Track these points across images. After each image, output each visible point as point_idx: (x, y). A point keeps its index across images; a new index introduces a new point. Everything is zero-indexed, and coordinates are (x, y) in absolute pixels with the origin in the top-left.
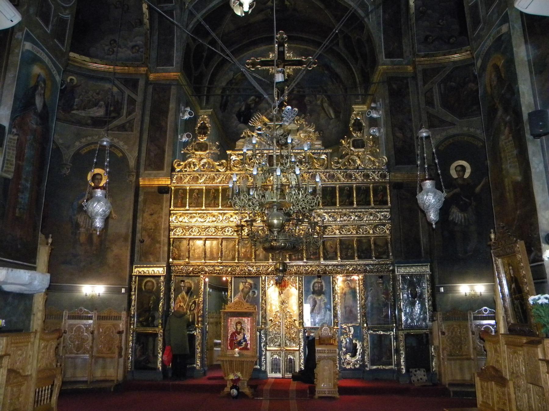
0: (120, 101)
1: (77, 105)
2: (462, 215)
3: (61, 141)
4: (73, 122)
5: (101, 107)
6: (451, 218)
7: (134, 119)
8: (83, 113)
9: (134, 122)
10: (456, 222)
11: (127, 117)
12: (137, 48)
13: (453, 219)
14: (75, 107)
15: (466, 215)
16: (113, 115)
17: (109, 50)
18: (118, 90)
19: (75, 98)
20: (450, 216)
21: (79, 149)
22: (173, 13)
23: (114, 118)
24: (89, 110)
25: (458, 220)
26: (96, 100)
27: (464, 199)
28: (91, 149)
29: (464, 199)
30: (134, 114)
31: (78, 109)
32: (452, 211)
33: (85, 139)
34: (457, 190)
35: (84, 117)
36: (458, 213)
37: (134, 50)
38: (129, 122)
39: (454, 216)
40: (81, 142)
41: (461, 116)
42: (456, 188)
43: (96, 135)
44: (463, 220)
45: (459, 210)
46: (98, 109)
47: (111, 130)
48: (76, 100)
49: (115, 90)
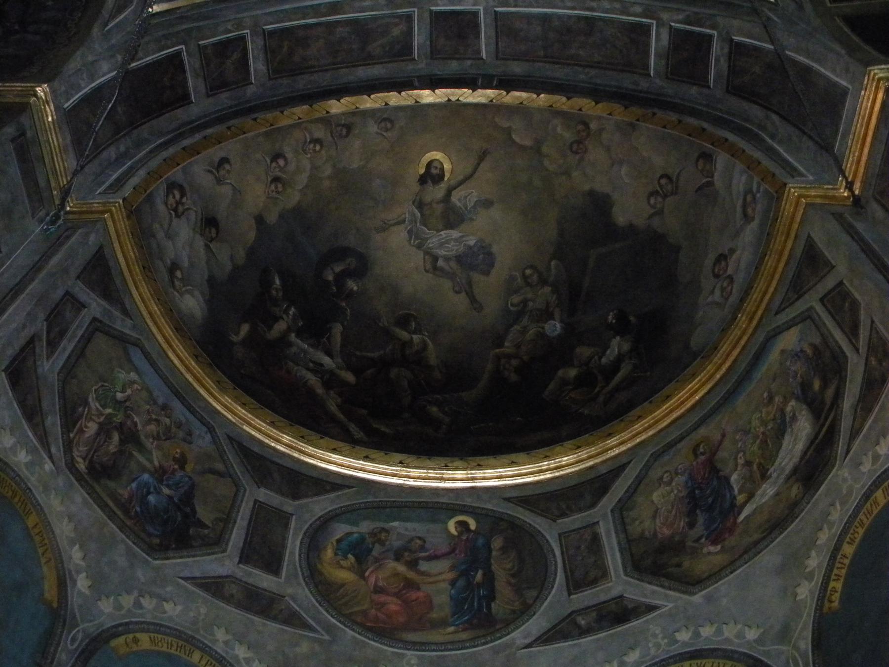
0: (817, 340)
1: (740, 492)
3: (752, 634)
4: (756, 543)
5: (794, 418)
7: (873, 322)
8: (767, 491)
9: (877, 332)
11: (857, 350)
12: (749, 198)
14: (741, 499)
16: (830, 392)
17: (723, 289)
18: (799, 326)
19: (727, 479)
21: (819, 607)
22: (739, 45)
23: (838, 395)
24: (777, 463)
26: (774, 419)
28: (847, 562)
30: (863, 316)
31: (751, 496)
33: (813, 554)
35: (777, 494)
37: (749, 211)
38: (871, 349)
40: (810, 577)
43: (833, 505)
46: (792, 430)
47: (854, 434)
48: (734, 478)
49: (790, 340)
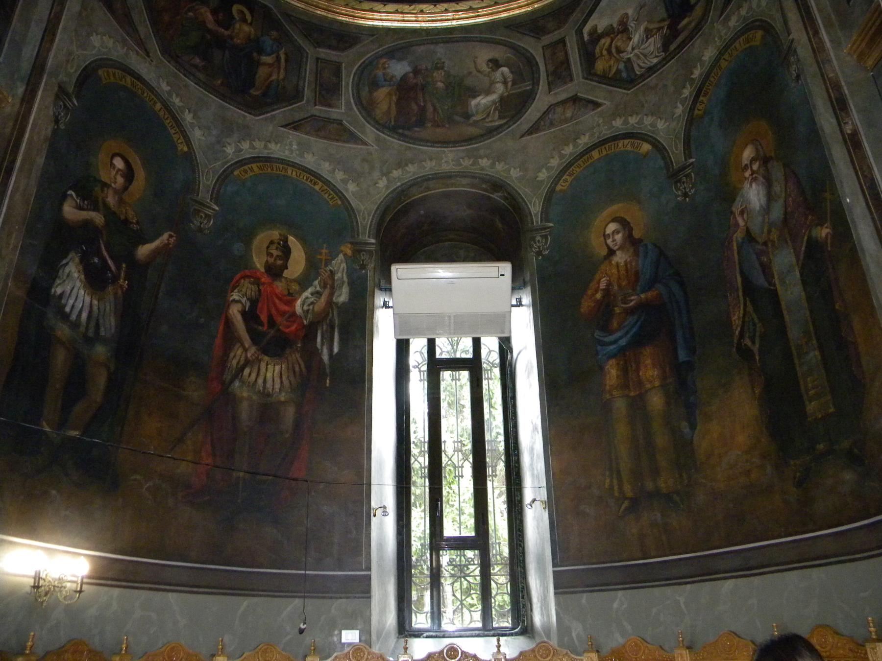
2: (88, 299)
6: (59, 291)
10: (68, 309)
13: (61, 296)
15: (95, 302)
20: (58, 281)
25: (73, 307)
27: (105, 253)
29: (105, 253)
32: (67, 270)
34: (98, 218)
36: (78, 284)
39: (68, 288)
41: (167, 51)
42: (96, 209)
44: (84, 315)
45: (83, 276)
